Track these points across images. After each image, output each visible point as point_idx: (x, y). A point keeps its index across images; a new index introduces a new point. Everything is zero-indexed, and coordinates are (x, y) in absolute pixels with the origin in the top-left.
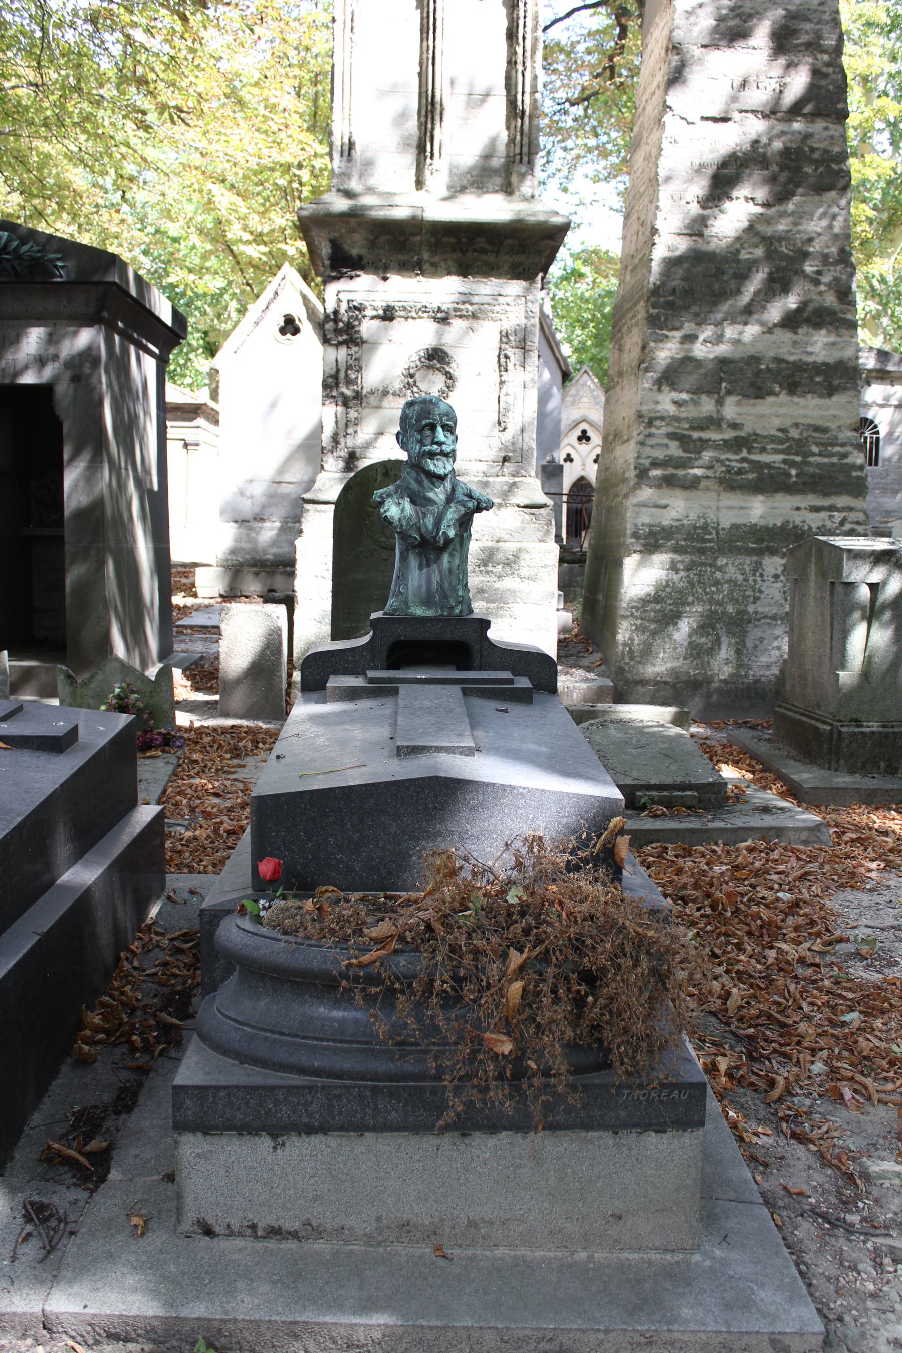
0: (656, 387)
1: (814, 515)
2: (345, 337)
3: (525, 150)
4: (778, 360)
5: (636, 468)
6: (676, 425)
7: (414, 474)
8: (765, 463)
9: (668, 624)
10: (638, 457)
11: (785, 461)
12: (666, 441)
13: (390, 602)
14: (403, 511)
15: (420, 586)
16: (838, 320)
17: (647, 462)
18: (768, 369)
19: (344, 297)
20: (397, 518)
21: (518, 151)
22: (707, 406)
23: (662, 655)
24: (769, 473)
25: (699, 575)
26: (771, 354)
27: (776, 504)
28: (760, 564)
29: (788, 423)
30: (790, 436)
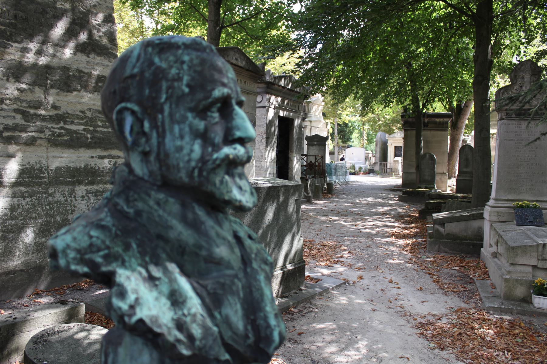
0: (5, 78)
4: (80, 71)
6: (19, 104)
7: (174, 205)
8: (74, 131)
9: (20, 232)
11: (84, 130)
12: (13, 114)
16: (109, 53)
18: (74, 76)
22: (39, 94)
23: (18, 253)
24: (77, 136)
25: (39, 199)
27: (81, 155)
28: (74, 190)
29: (85, 108)
30: (86, 115)
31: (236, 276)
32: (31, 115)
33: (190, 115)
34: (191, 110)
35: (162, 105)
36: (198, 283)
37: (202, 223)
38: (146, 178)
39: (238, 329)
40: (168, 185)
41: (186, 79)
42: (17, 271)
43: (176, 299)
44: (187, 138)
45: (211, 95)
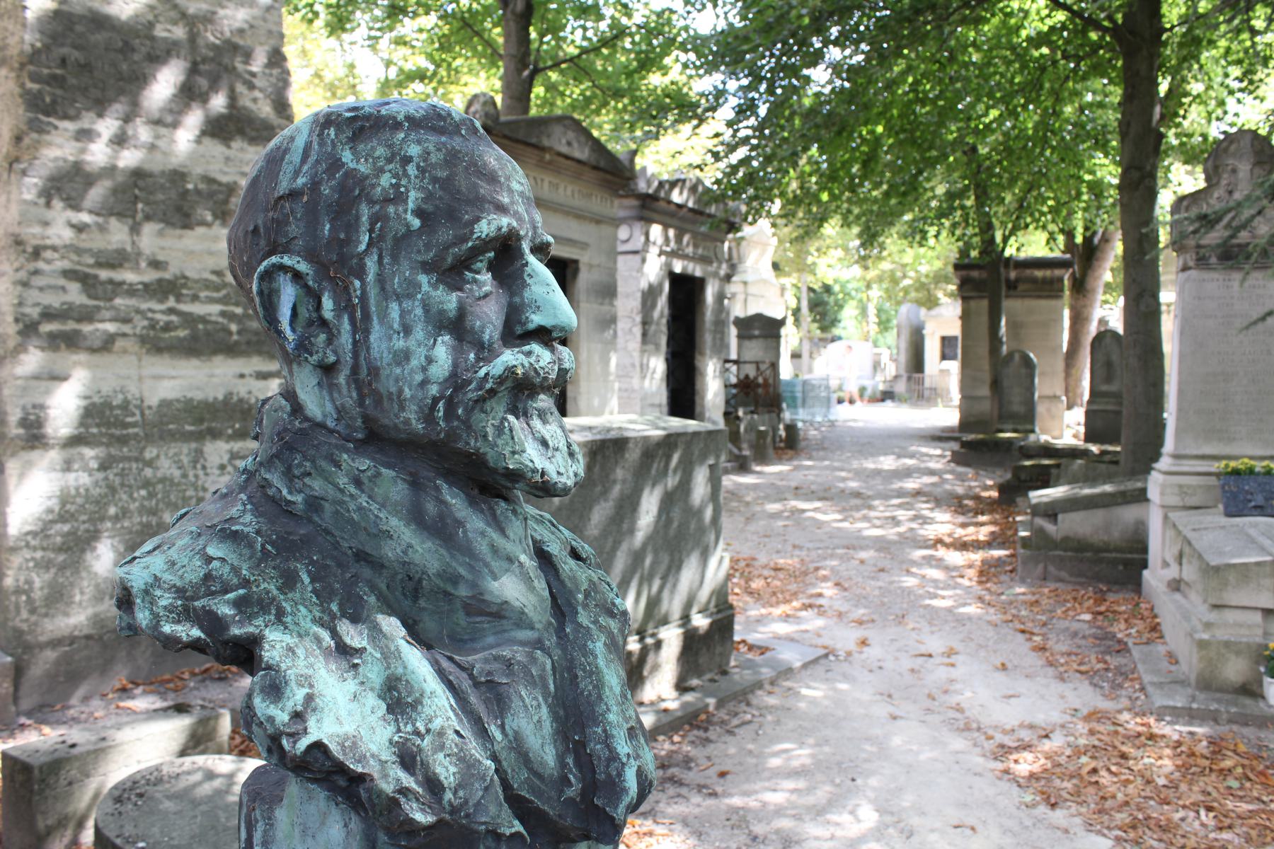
4: (210, 180)
5: (17, 320)
6: (75, 258)
7: (392, 485)
9: (83, 551)
10: (20, 304)
11: (223, 314)
12: (62, 282)
17: (34, 312)
18: (197, 191)
22: (118, 235)
23: (78, 598)
24: (205, 329)
25: (122, 474)
26: (198, 170)
31: (538, 644)
32: (102, 283)
33: (423, 279)
34: (427, 267)
35: (361, 257)
36: (451, 659)
37: (460, 523)
38: (330, 423)
39: (543, 763)
40: (377, 438)
41: (413, 197)
42: (76, 637)
43: (398, 699)
44: (419, 333)
45: (472, 233)
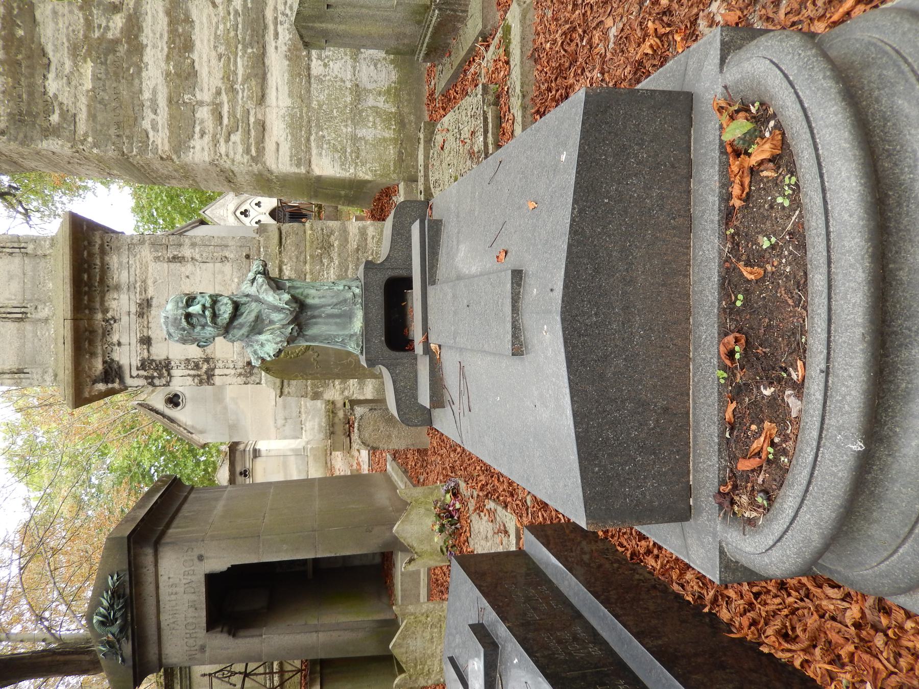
1: (280, 36)
2: (164, 370)
3: (16, 245)
12: (230, 143)
13: (350, 349)
14: (268, 341)
15: (336, 324)
16: (135, 13)
17: (246, 158)
19: (134, 373)
20: (275, 346)
21: (17, 250)
26: (163, 65)
29: (214, 53)
